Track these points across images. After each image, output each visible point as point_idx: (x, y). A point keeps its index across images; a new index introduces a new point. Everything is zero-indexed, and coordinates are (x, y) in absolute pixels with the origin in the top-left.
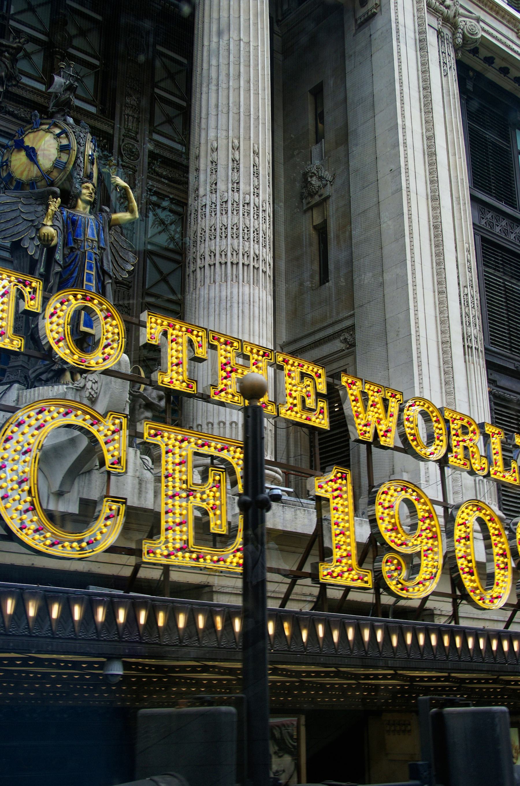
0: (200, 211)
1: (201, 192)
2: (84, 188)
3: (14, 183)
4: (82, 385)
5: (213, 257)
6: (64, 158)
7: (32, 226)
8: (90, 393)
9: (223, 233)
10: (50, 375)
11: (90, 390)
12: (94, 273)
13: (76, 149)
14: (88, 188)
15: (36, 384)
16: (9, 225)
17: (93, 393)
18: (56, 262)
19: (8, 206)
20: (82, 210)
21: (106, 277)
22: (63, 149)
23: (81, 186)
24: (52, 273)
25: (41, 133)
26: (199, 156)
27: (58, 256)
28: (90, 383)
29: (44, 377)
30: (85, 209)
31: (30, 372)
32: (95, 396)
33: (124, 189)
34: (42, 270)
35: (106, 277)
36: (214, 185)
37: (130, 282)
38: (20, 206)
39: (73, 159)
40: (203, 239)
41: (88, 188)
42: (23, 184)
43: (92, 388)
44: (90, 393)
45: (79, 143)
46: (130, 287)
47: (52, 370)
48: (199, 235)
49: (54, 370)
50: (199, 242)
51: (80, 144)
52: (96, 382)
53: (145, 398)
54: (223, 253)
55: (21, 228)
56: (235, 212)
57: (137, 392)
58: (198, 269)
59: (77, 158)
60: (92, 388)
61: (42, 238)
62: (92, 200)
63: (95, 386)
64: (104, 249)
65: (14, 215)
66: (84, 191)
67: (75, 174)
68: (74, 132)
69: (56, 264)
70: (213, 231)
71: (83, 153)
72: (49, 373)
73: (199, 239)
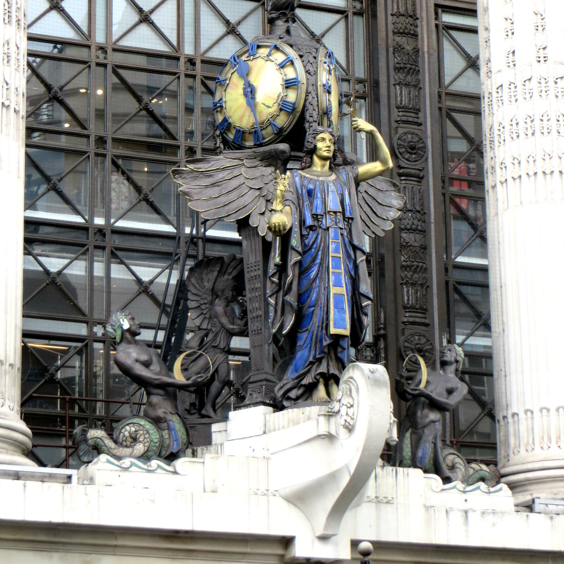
0: (495, 95)
1: (494, 66)
2: (318, 140)
3: (234, 131)
4: (336, 409)
5: (517, 164)
6: (292, 96)
7: (260, 196)
8: (346, 421)
9: (529, 128)
10: (300, 391)
11: (346, 417)
12: (341, 255)
13: (305, 82)
14: (323, 139)
15: (285, 403)
16: (232, 196)
17: (349, 419)
18: (293, 248)
19: (228, 172)
20: (319, 169)
21: (359, 253)
22: (289, 84)
23: (315, 138)
24: (291, 263)
25: (260, 62)
26: (488, 8)
27: (295, 242)
28: (345, 407)
29: (293, 394)
30: (323, 166)
31: (277, 388)
32: (352, 423)
33: (370, 135)
34: (278, 260)
35: (359, 253)
36: (511, 55)
37: (420, 170)
38: (243, 170)
39: (303, 96)
40: (502, 138)
41: (323, 139)
42: (244, 132)
43: (347, 414)
44: (346, 421)
45: (307, 72)
46: (422, 178)
47: (302, 385)
48: (496, 132)
49: (305, 386)
50: (496, 144)
51: (309, 74)
52: (352, 406)
53: (428, 397)
54: (531, 160)
55: (247, 199)
56: (544, 94)
57: (416, 390)
58: (499, 185)
59: (308, 93)
60: (347, 414)
61: (273, 229)
62: (330, 155)
63: (350, 411)
64: (352, 219)
65: (235, 183)
66: (320, 145)
67: (307, 117)
68: (301, 56)
69: (294, 252)
70: (514, 125)
71: (315, 85)
72: (299, 389)
73: (496, 139)
